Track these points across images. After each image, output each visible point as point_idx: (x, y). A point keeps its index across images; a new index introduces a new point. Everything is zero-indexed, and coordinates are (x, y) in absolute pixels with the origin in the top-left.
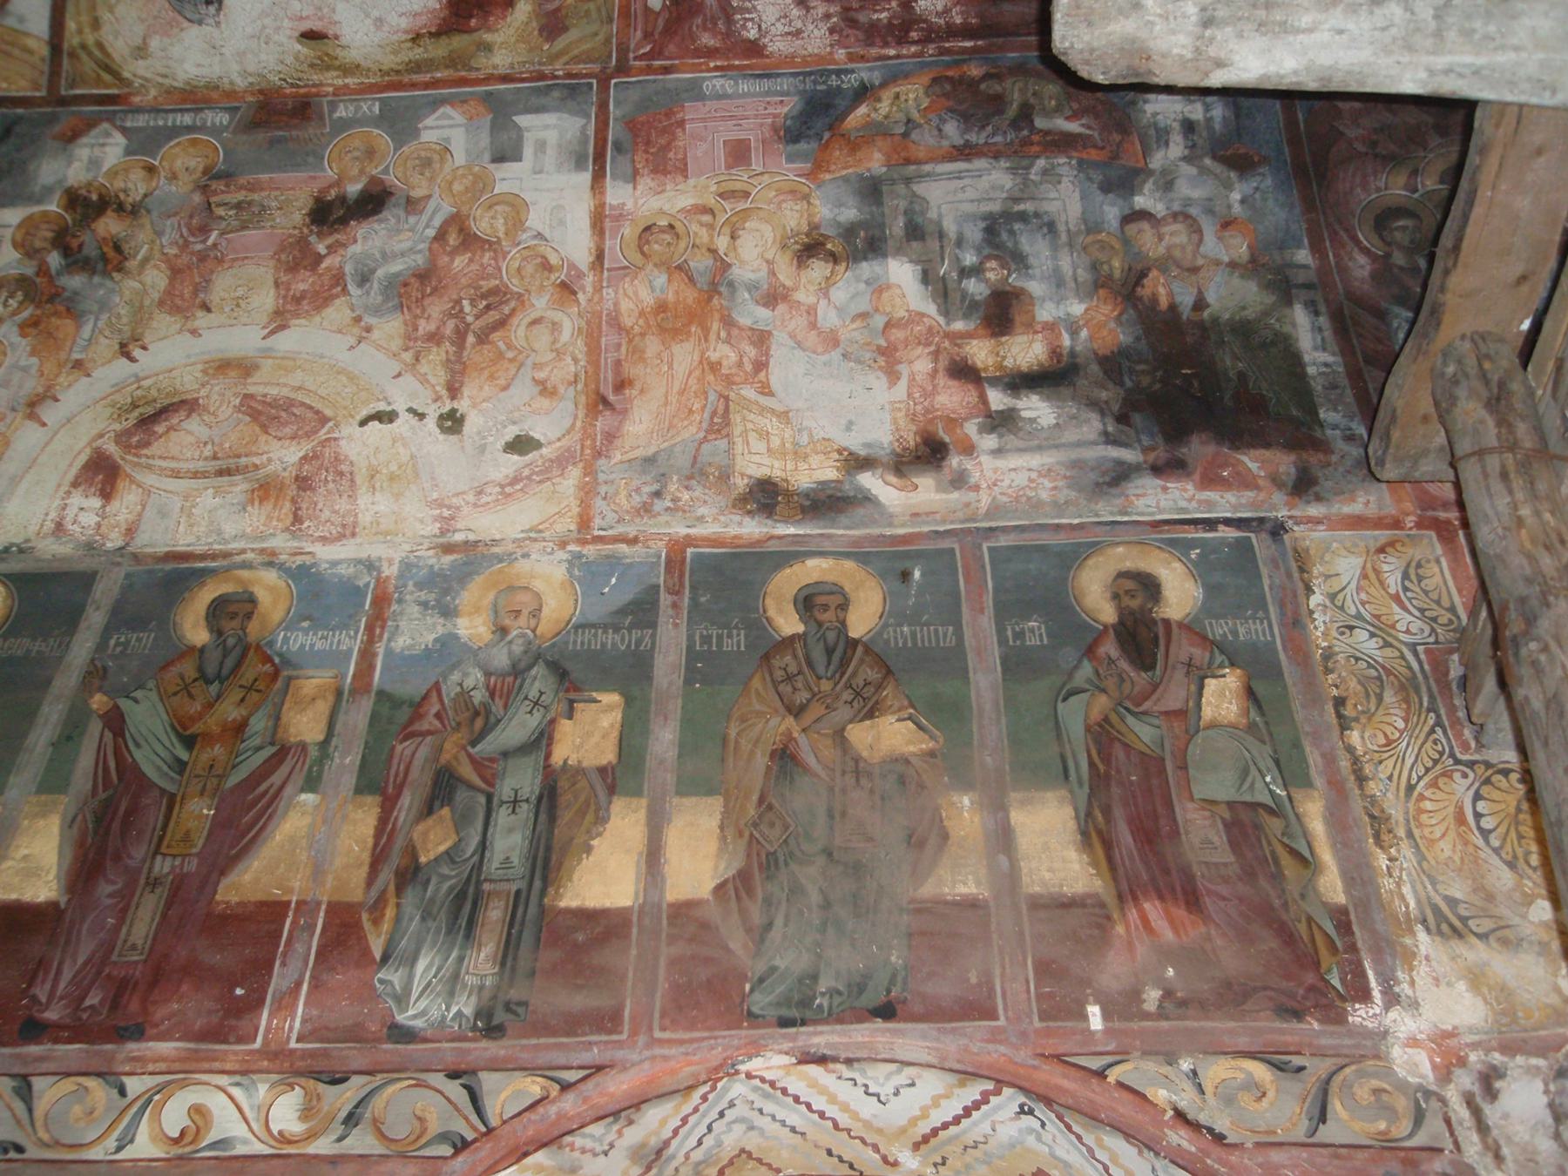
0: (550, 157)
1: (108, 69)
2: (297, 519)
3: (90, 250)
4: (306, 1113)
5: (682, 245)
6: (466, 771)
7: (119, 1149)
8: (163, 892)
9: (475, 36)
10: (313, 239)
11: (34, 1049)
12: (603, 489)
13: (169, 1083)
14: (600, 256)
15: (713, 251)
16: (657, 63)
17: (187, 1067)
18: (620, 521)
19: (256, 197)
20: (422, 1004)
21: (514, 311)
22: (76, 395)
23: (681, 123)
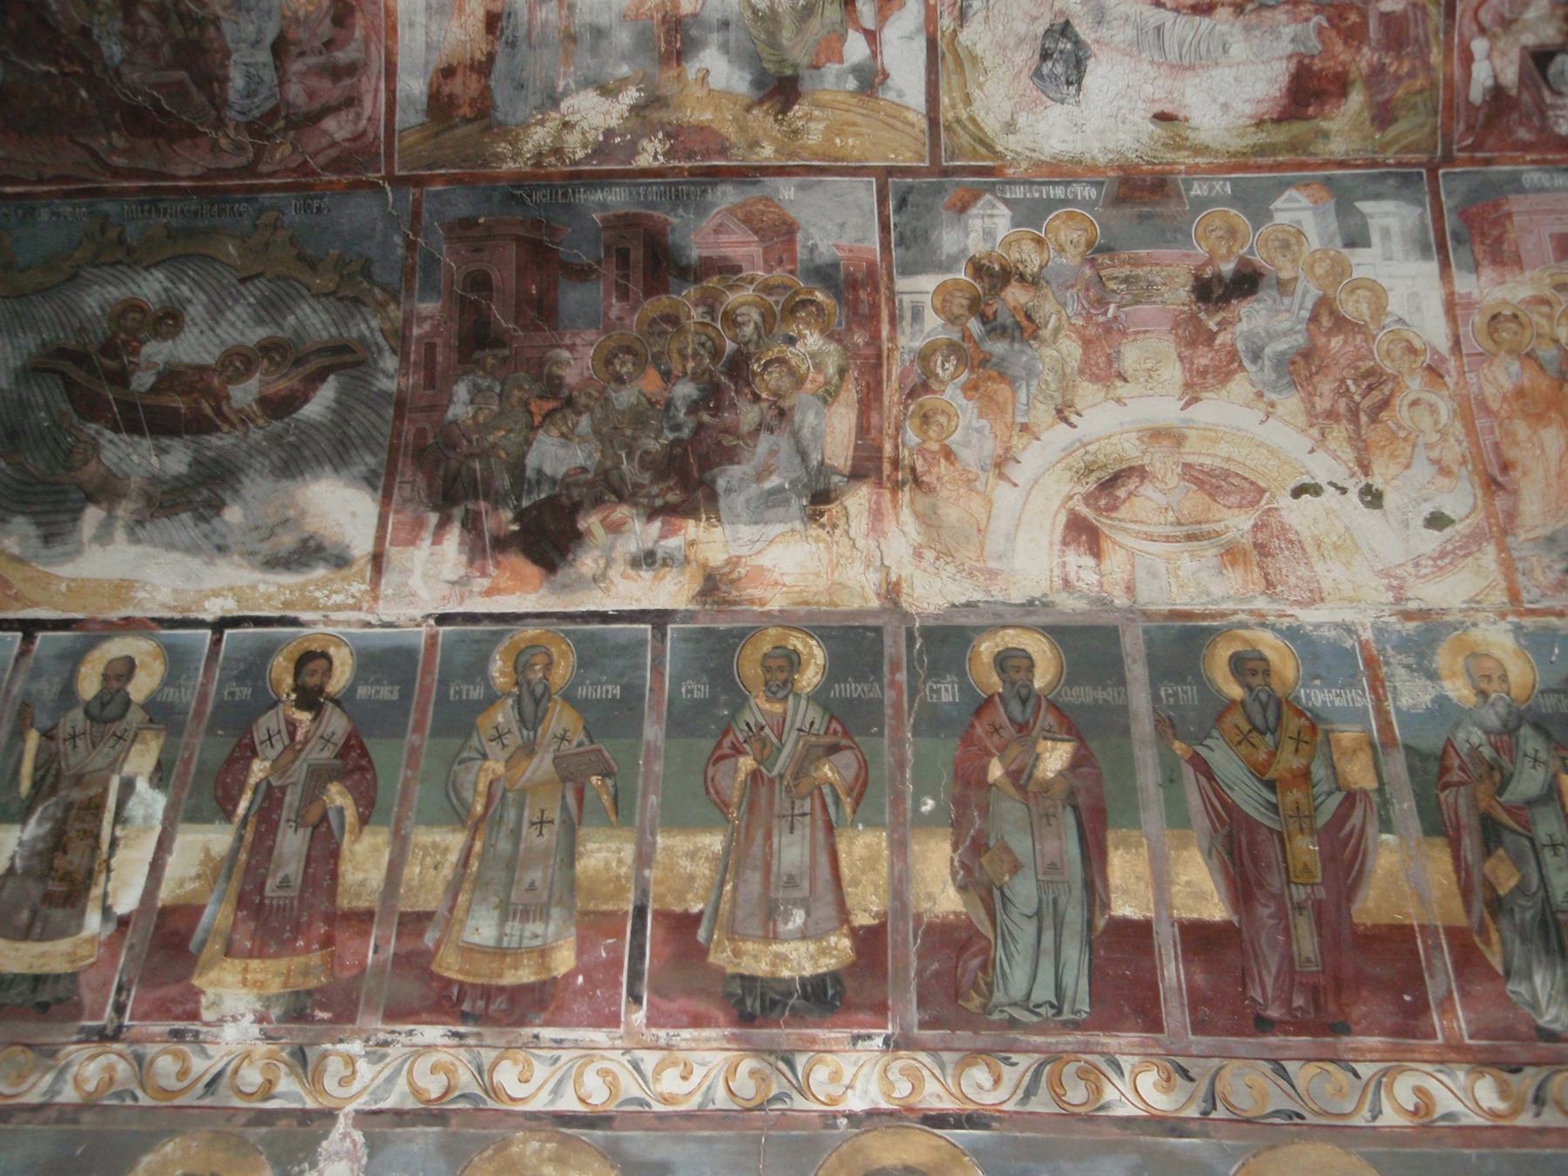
0: (1397, 246)
1: (982, 142)
2: (1270, 584)
3: (1004, 318)
4: (1504, 1094)
5: (1528, 334)
6: (1505, 819)
7: (1374, 1118)
8: (1309, 912)
9: (1313, 123)
10: (1202, 316)
11: (1271, 1040)
12: (1520, 565)
13: (1389, 1068)
14: (1457, 343)
15: (1556, 341)
16: (1479, 155)
17: (1398, 1056)
18: (1544, 595)
19: (1140, 272)
20: (1553, 1012)
21: (1392, 392)
22: (1033, 458)
23: (1509, 215)
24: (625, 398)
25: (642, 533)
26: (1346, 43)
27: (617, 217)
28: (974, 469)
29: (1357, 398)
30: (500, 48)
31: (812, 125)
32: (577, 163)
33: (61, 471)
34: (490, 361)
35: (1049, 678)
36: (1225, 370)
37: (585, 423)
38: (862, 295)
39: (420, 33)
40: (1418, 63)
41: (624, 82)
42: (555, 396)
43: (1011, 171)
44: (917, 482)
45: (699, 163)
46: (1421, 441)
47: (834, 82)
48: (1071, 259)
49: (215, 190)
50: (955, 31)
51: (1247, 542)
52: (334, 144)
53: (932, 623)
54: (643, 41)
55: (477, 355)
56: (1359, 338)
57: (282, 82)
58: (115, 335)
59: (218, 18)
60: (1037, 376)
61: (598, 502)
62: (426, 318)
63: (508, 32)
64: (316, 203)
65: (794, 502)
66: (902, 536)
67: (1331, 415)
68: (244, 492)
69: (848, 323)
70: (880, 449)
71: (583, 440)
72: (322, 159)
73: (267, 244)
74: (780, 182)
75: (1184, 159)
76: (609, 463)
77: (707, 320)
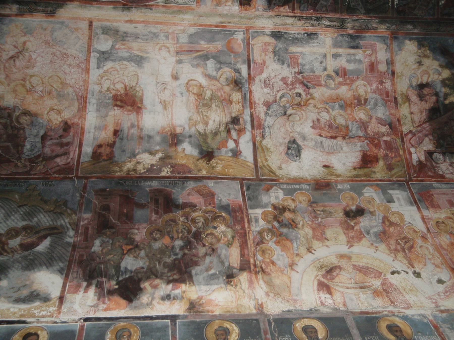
0: (403, 202)
1: (272, 172)
2: (392, 302)
3: (285, 222)
5: (448, 227)
9: (370, 169)
14: (428, 230)
16: (419, 179)
22: (302, 264)
24: (157, 245)
25: (165, 289)
26: (375, 148)
27: (155, 190)
28: (282, 267)
29: (403, 245)
31: (218, 165)
32: (140, 174)
34: (108, 233)
35: (323, 335)
36: (360, 236)
37: (142, 253)
38: (238, 214)
39: (92, 135)
40: (397, 154)
41: (157, 151)
42: (132, 245)
43: (281, 180)
44: (263, 271)
45: (181, 175)
46: (426, 257)
47: (224, 153)
48: (304, 205)
50: (261, 141)
51: (380, 288)
52: (58, 166)
53: (277, 317)
54: (164, 140)
55: (104, 231)
56: (398, 228)
57: (43, 147)
59: (25, 128)
60: (299, 239)
61: (148, 278)
62: (85, 219)
64: (50, 183)
65: (220, 277)
66: (260, 290)
67: (396, 250)
69: (233, 222)
70: (249, 261)
71: (142, 258)
72: (54, 170)
73: (30, 195)
74: (208, 181)
75: (334, 178)
76: (152, 266)
77: (186, 221)
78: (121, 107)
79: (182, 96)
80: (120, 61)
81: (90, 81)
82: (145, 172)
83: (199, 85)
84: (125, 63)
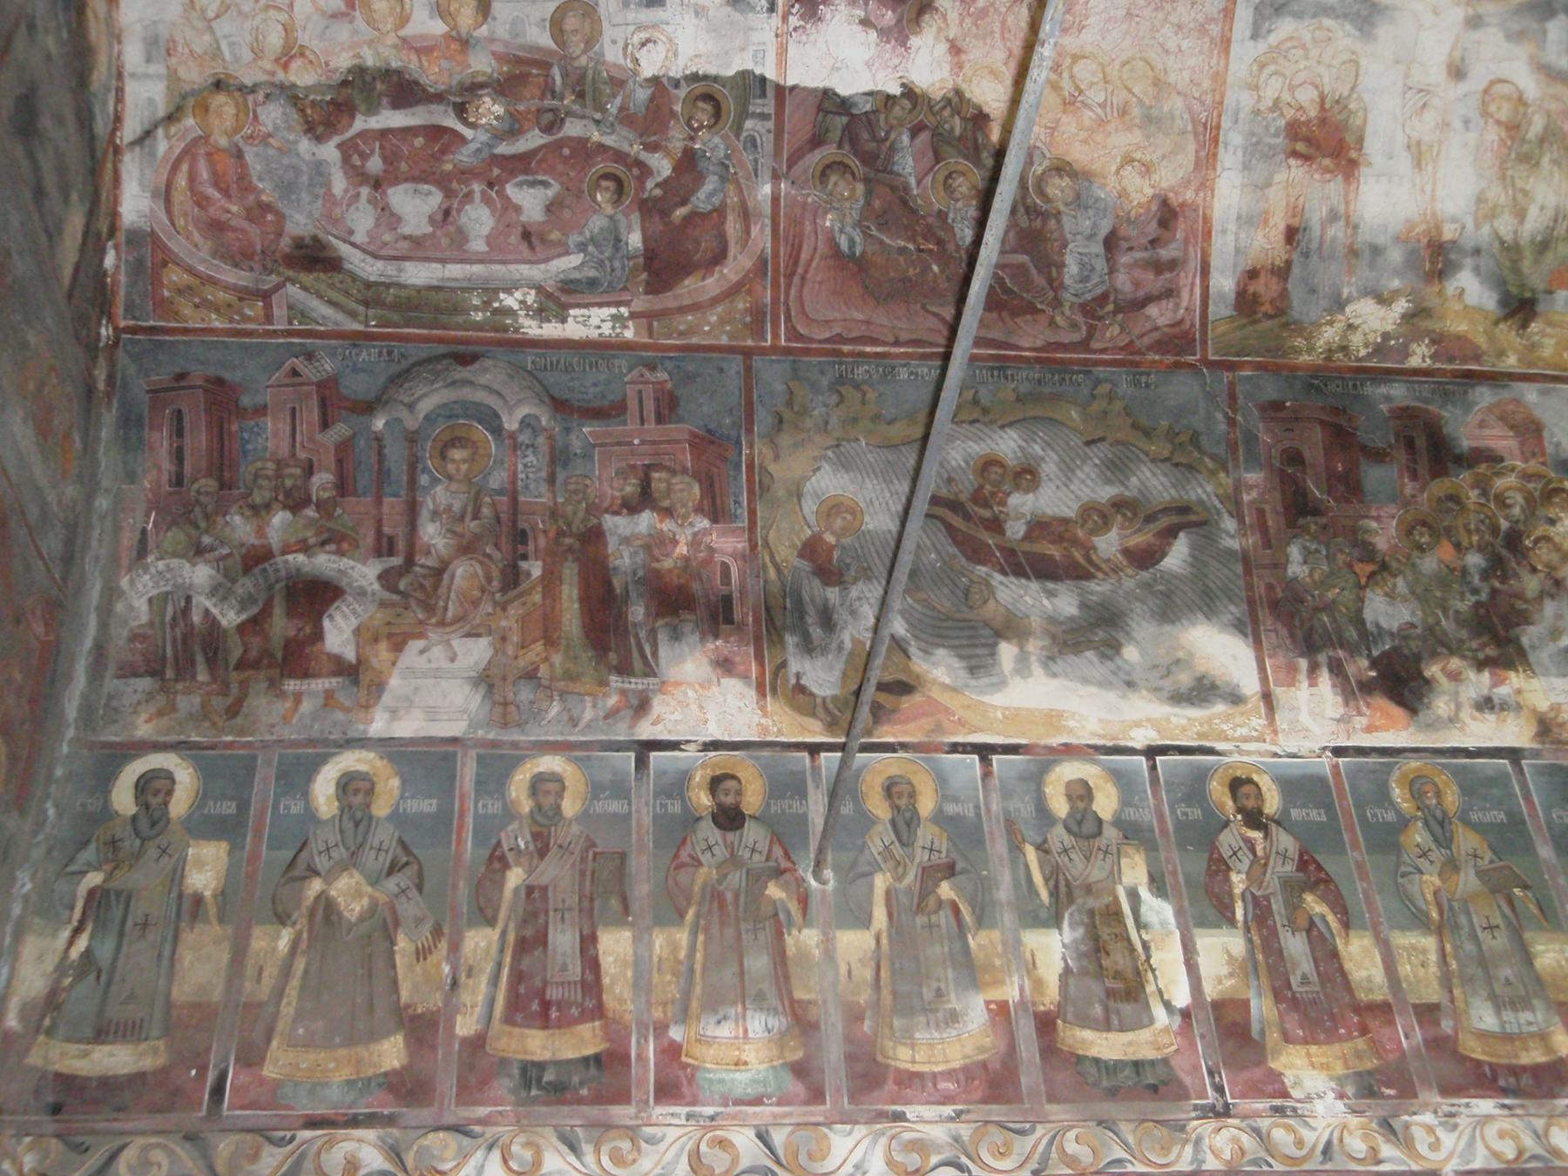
25: (1478, 683)
30: (1295, 256)
32: (1359, 360)
33: (965, 609)
34: (1313, 527)
37: (1401, 584)
39: (1230, 238)
41: (1396, 294)
49: (1054, 361)
52: (1156, 329)
54: (1411, 261)
55: (1301, 521)
57: (1112, 271)
58: (981, 487)
61: (1434, 655)
63: (1303, 244)
64: (1143, 379)
68: (1135, 634)
72: (1147, 341)
74: (1524, 386)
76: (1431, 620)
77: (1483, 501)
78: (1307, 158)
79: (1467, 129)
80: (1315, 16)
81: (1230, 80)
82: (1369, 356)
83: (1515, 96)
84: (1328, 22)
